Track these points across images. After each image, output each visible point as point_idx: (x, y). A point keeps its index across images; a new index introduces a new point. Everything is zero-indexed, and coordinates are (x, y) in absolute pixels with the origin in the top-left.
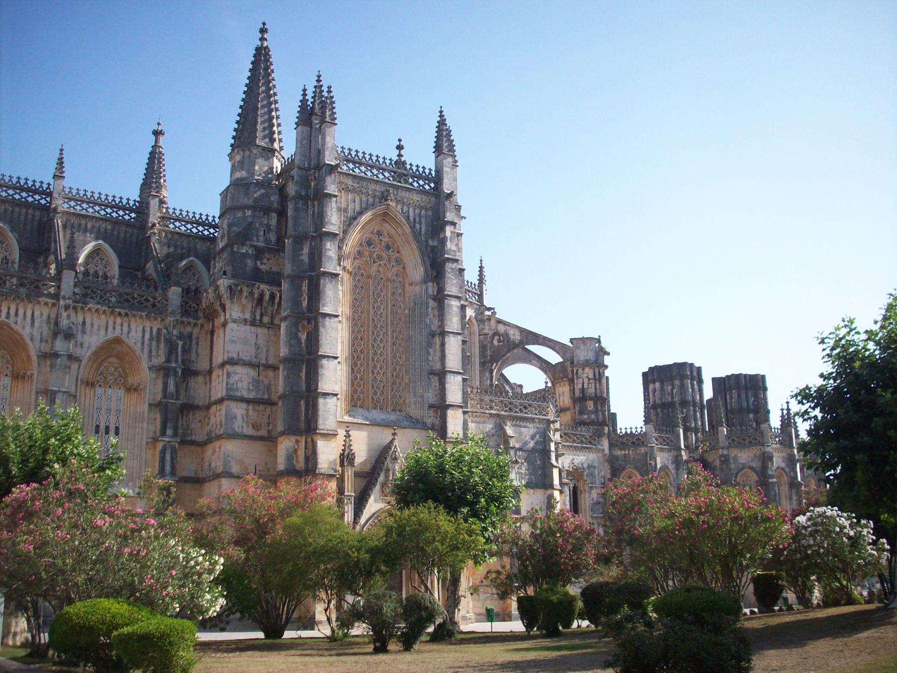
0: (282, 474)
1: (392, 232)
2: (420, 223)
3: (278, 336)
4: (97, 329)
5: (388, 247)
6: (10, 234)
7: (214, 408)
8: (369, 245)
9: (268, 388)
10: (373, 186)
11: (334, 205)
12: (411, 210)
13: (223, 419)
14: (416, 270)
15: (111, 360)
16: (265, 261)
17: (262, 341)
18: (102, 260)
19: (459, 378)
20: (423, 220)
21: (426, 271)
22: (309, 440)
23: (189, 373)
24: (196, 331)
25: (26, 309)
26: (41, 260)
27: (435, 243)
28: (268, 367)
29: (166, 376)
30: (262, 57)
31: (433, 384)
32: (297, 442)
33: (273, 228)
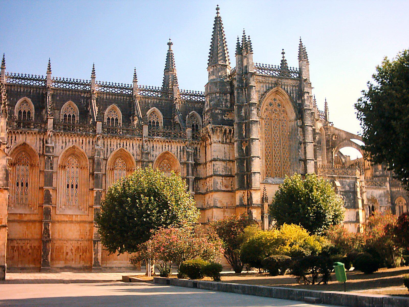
0: (237, 206)
2: (293, 93)
3: (233, 147)
4: (158, 147)
5: (279, 105)
6: (118, 108)
7: (208, 179)
8: (271, 105)
10: (271, 79)
11: (254, 90)
12: (289, 88)
13: (213, 184)
14: (292, 115)
15: (165, 160)
16: (226, 115)
17: (227, 150)
18: (156, 116)
19: (313, 162)
20: (294, 92)
21: (296, 115)
22: (249, 192)
23: (197, 164)
24: (199, 146)
26: (131, 118)
27: (300, 102)
28: (230, 161)
29: (188, 167)
31: (301, 165)
32: (244, 193)
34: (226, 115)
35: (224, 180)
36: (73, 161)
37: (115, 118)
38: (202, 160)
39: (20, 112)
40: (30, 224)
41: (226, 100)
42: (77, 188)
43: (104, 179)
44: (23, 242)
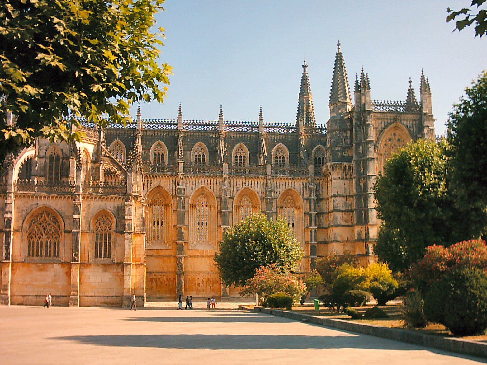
1: (400, 133)
2: (413, 127)
4: (282, 185)
5: (399, 140)
6: (245, 146)
7: (330, 214)
9: (351, 205)
10: (390, 115)
12: (408, 122)
15: (288, 197)
16: (346, 152)
17: (347, 186)
18: (282, 151)
20: (414, 126)
23: (319, 199)
24: (321, 182)
25: (254, 181)
26: (258, 155)
28: (350, 196)
29: (310, 203)
30: (339, 58)
32: (362, 228)
33: (349, 137)
34: (346, 152)
35: (344, 215)
36: (203, 200)
37: (242, 156)
38: (324, 195)
39: (155, 155)
40: (166, 258)
41: (346, 137)
42: (206, 225)
43: (231, 217)
44: (160, 274)
